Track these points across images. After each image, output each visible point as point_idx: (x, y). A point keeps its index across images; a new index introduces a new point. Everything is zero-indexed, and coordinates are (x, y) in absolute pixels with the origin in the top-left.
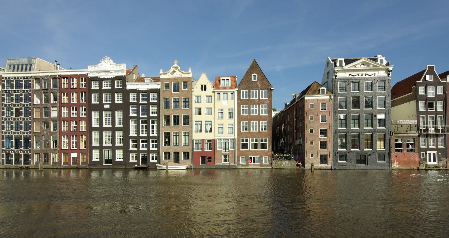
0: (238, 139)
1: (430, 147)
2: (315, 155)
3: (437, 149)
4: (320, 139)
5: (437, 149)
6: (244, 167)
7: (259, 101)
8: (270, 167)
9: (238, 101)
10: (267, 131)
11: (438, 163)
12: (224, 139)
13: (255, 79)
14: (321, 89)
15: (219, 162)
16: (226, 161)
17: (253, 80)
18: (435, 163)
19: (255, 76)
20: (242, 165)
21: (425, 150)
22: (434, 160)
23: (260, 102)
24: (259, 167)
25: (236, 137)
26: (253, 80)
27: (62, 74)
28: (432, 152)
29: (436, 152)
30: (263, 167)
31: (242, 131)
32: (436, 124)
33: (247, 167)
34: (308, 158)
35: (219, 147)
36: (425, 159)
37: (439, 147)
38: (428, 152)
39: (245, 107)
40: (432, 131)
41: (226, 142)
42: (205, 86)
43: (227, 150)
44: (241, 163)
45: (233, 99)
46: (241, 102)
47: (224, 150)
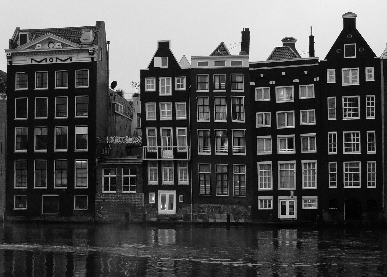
1: (164, 183)
3: (176, 187)
5: (176, 187)
11: (177, 211)
18: (173, 212)
21: (155, 189)
22: (171, 208)
28: (167, 194)
29: (174, 193)
32: (175, 144)
36: (155, 206)
37: (180, 183)
38: (161, 193)
40: (168, 155)
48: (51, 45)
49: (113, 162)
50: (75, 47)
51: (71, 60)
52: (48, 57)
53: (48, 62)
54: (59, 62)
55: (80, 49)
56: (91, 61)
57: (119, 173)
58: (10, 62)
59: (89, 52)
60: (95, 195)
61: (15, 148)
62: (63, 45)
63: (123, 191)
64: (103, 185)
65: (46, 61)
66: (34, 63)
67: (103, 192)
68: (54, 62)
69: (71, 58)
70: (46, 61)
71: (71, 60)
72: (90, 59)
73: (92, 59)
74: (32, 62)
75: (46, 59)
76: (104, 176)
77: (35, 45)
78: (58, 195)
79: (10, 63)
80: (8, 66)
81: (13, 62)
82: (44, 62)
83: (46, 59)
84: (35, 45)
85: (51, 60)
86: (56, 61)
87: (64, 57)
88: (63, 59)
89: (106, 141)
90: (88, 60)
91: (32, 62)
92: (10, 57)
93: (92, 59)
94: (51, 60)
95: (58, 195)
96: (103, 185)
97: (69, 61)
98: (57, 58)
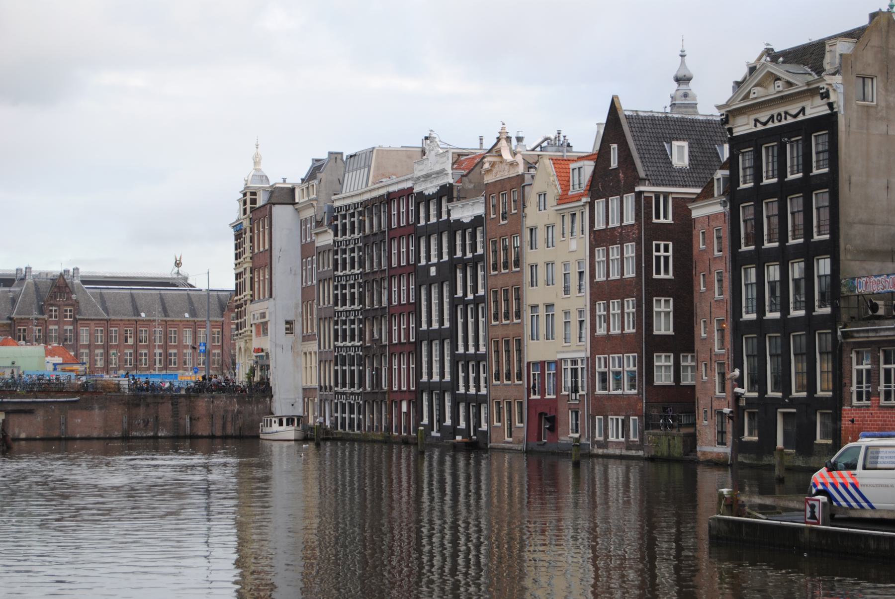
2: (709, 414)
6: (600, 451)
8: (641, 453)
24: (624, 452)
25: (589, 355)
27: (392, 189)
49: (862, 335)
50: (801, 85)
51: (804, 114)
52: (775, 112)
53: (777, 124)
54: (790, 120)
55: (806, 88)
56: (829, 112)
57: (875, 361)
59: (822, 94)
60: (841, 410)
61: (744, 310)
62: (789, 84)
63: (882, 402)
64: (854, 388)
66: (760, 127)
67: (855, 402)
68: (784, 122)
71: (804, 114)
72: (827, 107)
73: (830, 105)
74: (755, 126)
75: (772, 117)
76: (855, 367)
77: (749, 93)
78: (794, 410)
81: (734, 130)
82: (770, 125)
84: (749, 93)
86: (786, 118)
87: (794, 109)
89: (855, 287)
90: (824, 110)
91: (755, 126)
93: (830, 105)
95: (794, 410)
96: (854, 388)
97: (801, 118)
98: (786, 113)
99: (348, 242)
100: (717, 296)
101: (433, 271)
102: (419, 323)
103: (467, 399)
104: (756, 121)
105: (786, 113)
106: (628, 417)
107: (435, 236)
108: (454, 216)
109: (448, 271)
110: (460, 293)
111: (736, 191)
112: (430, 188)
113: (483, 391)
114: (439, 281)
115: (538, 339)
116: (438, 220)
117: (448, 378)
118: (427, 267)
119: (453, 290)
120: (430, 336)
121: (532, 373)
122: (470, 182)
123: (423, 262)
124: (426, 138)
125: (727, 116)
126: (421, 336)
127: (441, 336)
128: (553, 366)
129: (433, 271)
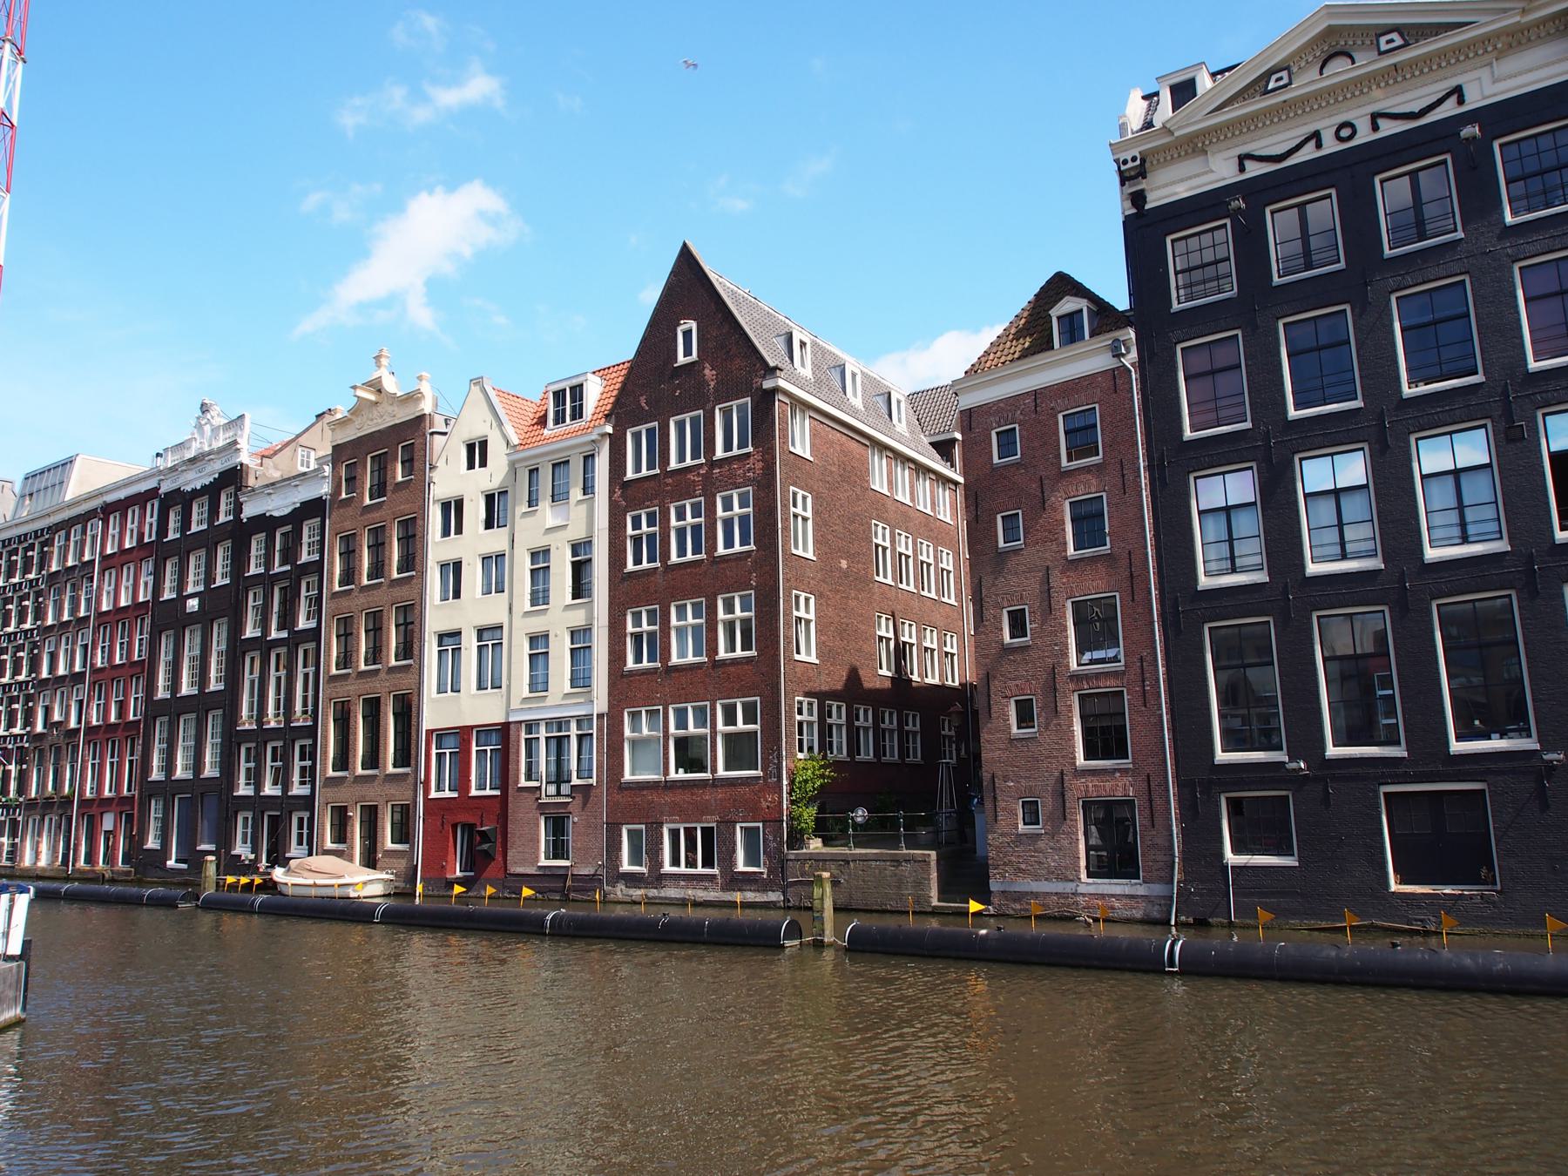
0: (613, 719)
4: (1076, 678)
7: (707, 477)
8: (774, 896)
9: (611, 492)
10: (753, 653)
12: (549, 723)
13: (688, 352)
14: (1055, 312)
15: (523, 862)
16: (558, 850)
17: (681, 359)
19: (687, 334)
20: (632, 880)
23: (707, 481)
26: (681, 359)
30: (738, 897)
31: (630, 664)
33: (653, 893)
34: (1005, 825)
35: (534, 769)
39: (640, 526)
41: (560, 740)
42: (484, 444)
43: (565, 789)
44: (626, 866)
45: (588, 488)
46: (626, 496)
47: (552, 789)
48: (1339, 66)
51: (1461, 102)
53: (1331, 146)
54: (1388, 128)
58: (1138, 199)
65: (1319, 146)
66: (1254, 170)
68: (1364, 136)
69: (1458, 92)
70: (1319, 146)
71: (1461, 102)
74: (1242, 169)
75: (1316, 136)
79: (1134, 204)
80: (1128, 223)
81: (1150, 197)
82: (1308, 153)
83: (1316, 136)
85: (1345, 133)
86: (1375, 128)
88: (1416, 107)
91: (1242, 169)
92: (1132, 174)
94: (1345, 133)
97: (1449, 109)
98: (1375, 117)
99: (16, 588)
100: (1071, 550)
101: (193, 604)
102: (151, 687)
103: (258, 803)
104: (1242, 159)
105: (1375, 117)
106: (729, 824)
107: (203, 553)
108: (249, 511)
109: (224, 605)
110: (250, 632)
111: (1249, 283)
112: (194, 480)
113: (297, 790)
114: (204, 620)
115: (456, 690)
116: (211, 523)
117: (210, 771)
118: (182, 599)
119: (236, 627)
120: (176, 707)
121: (434, 751)
122: (276, 468)
123: (168, 595)
124: (158, 455)
125: (1143, 161)
126: (154, 709)
127: (201, 704)
128: (450, 741)
129: (193, 604)
